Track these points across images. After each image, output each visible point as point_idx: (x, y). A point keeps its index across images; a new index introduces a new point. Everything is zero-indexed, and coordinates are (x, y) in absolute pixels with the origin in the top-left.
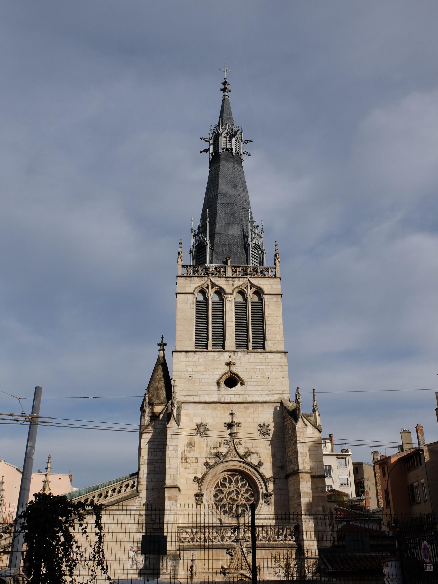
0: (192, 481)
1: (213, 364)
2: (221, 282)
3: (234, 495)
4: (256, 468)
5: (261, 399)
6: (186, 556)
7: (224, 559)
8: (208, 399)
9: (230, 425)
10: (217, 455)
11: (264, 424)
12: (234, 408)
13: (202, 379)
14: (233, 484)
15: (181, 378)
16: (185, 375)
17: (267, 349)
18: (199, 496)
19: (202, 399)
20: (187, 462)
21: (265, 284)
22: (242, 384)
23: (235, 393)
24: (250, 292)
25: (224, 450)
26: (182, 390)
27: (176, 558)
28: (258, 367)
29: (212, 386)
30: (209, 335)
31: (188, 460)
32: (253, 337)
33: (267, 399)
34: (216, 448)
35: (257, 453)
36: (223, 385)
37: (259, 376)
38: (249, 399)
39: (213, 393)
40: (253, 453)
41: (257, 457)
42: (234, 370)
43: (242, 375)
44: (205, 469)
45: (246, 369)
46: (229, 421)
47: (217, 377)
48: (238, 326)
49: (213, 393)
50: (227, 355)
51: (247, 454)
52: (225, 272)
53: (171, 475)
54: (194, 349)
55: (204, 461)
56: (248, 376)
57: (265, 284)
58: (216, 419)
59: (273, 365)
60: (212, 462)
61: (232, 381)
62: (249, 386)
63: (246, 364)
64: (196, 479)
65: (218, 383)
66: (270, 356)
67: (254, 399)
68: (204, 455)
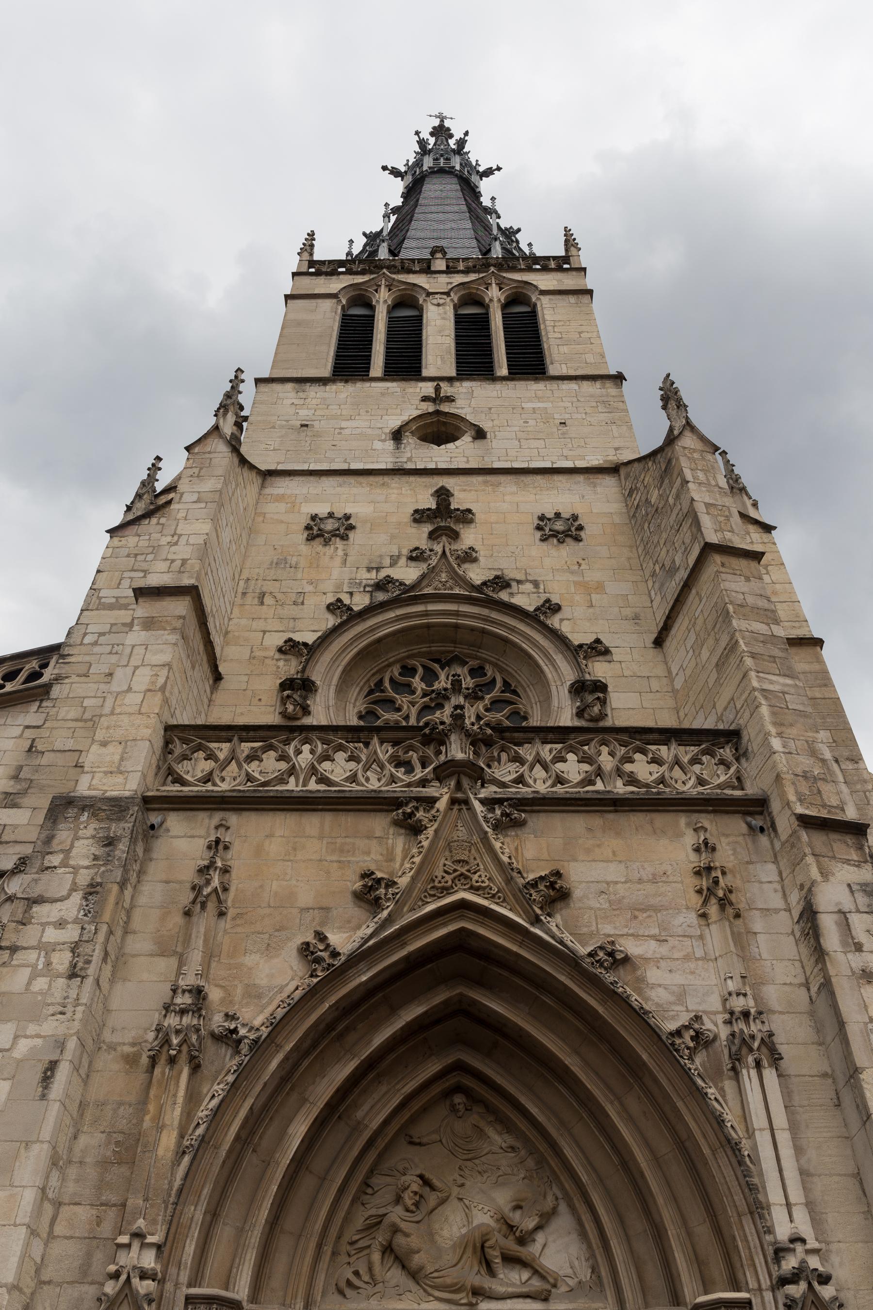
0: (272, 652)
11: (558, 515)
12: (448, 482)
13: (341, 428)
15: (274, 427)
16: (287, 421)
20: (262, 603)
26: (274, 450)
28: (528, 405)
29: (376, 442)
31: (268, 600)
34: (378, 569)
35: (536, 584)
37: (532, 422)
40: (519, 582)
41: (535, 590)
45: (490, 409)
53: (173, 561)
55: (330, 599)
56: (496, 422)
59: (578, 400)
64: (291, 648)
68: (329, 586)
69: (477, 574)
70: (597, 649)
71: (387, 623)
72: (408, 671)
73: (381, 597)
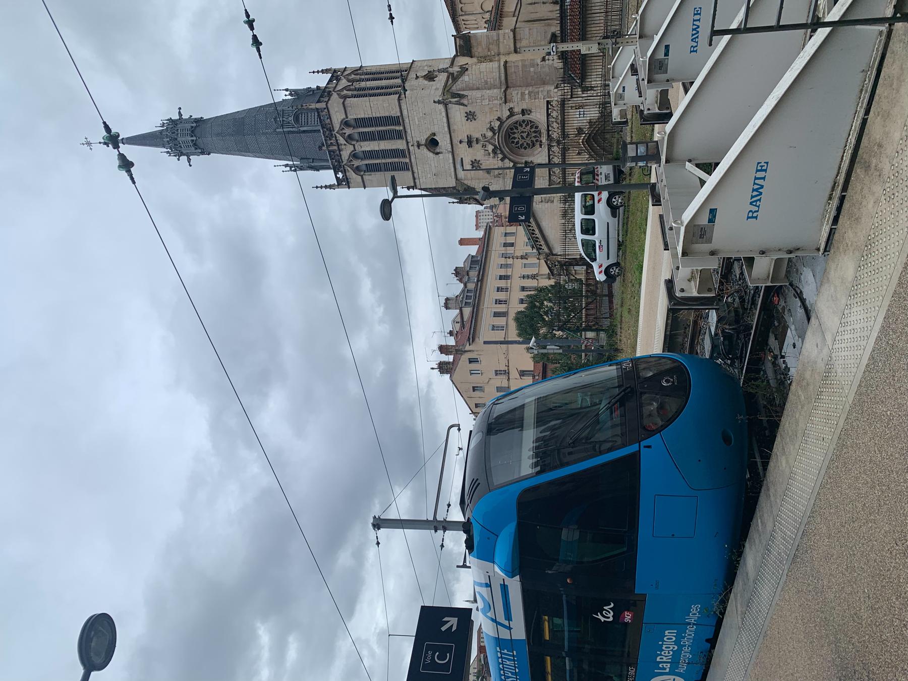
1: (422, 158)
2: (345, 154)
3: (525, 135)
4: (502, 123)
5: (445, 119)
8: (451, 161)
9: (470, 143)
10: (494, 151)
14: (516, 136)
17: (399, 114)
19: (452, 165)
22: (434, 134)
23: (444, 142)
33: (444, 114)
36: (438, 150)
38: (446, 129)
42: (423, 142)
44: (507, 161)
46: (465, 145)
47: (431, 155)
50: (411, 148)
51: (492, 129)
52: (334, 151)
54: (410, 173)
58: (466, 154)
60: (500, 156)
61: (432, 143)
62: (435, 129)
63: (417, 132)
65: (437, 154)
66: (405, 113)
67: (446, 125)
69: (489, 134)
70: (511, 110)
71: (506, 150)
72: (513, 142)
73: (499, 152)
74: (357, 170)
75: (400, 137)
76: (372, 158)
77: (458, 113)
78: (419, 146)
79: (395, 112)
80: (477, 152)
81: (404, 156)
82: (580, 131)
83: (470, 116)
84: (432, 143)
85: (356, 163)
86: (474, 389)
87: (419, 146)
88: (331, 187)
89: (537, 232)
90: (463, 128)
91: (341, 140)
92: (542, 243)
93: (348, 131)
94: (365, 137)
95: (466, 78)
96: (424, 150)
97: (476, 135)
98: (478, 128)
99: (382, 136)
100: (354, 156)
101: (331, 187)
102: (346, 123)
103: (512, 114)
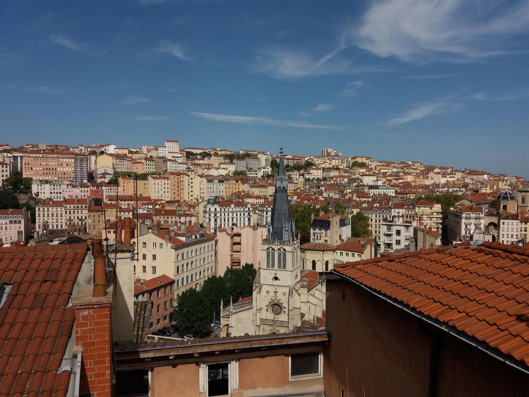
2: (274, 247)
4: (281, 304)
6: (262, 326)
7: (271, 328)
10: (272, 300)
18: (267, 310)
21: (287, 248)
23: (276, 282)
24: (282, 250)
25: (274, 298)
27: (259, 326)
30: (270, 263)
32: (283, 265)
36: (274, 280)
39: (271, 282)
42: (277, 276)
43: (279, 277)
48: (279, 261)
49: (271, 282)
51: (279, 300)
57: (287, 248)
58: (272, 289)
61: (276, 278)
71: (272, 303)
74: (268, 249)
75: (279, 267)
76: (272, 255)
77: (287, 290)
78: (276, 274)
79: (287, 268)
80: (272, 294)
81: (272, 267)
82: (278, 331)
83: (284, 294)
84: (276, 278)
85: (271, 249)
86: (144, 243)
87: (276, 274)
88: (262, 237)
89: (241, 309)
90: (281, 291)
91: (279, 247)
92: (237, 310)
93: (282, 250)
94: (279, 255)
95: (297, 295)
96: (274, 275)
97: (278, 294)
98: (280, 296)
99: (279, 261)
100: (273, 249)
101: (262, 237)
102: (285, 250)
103: (284, 308)
